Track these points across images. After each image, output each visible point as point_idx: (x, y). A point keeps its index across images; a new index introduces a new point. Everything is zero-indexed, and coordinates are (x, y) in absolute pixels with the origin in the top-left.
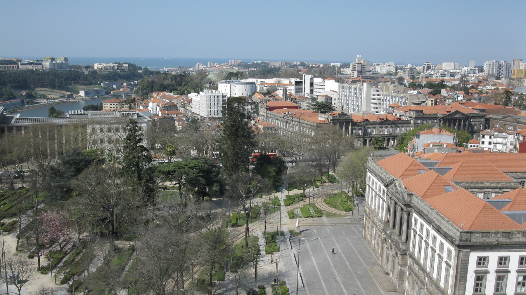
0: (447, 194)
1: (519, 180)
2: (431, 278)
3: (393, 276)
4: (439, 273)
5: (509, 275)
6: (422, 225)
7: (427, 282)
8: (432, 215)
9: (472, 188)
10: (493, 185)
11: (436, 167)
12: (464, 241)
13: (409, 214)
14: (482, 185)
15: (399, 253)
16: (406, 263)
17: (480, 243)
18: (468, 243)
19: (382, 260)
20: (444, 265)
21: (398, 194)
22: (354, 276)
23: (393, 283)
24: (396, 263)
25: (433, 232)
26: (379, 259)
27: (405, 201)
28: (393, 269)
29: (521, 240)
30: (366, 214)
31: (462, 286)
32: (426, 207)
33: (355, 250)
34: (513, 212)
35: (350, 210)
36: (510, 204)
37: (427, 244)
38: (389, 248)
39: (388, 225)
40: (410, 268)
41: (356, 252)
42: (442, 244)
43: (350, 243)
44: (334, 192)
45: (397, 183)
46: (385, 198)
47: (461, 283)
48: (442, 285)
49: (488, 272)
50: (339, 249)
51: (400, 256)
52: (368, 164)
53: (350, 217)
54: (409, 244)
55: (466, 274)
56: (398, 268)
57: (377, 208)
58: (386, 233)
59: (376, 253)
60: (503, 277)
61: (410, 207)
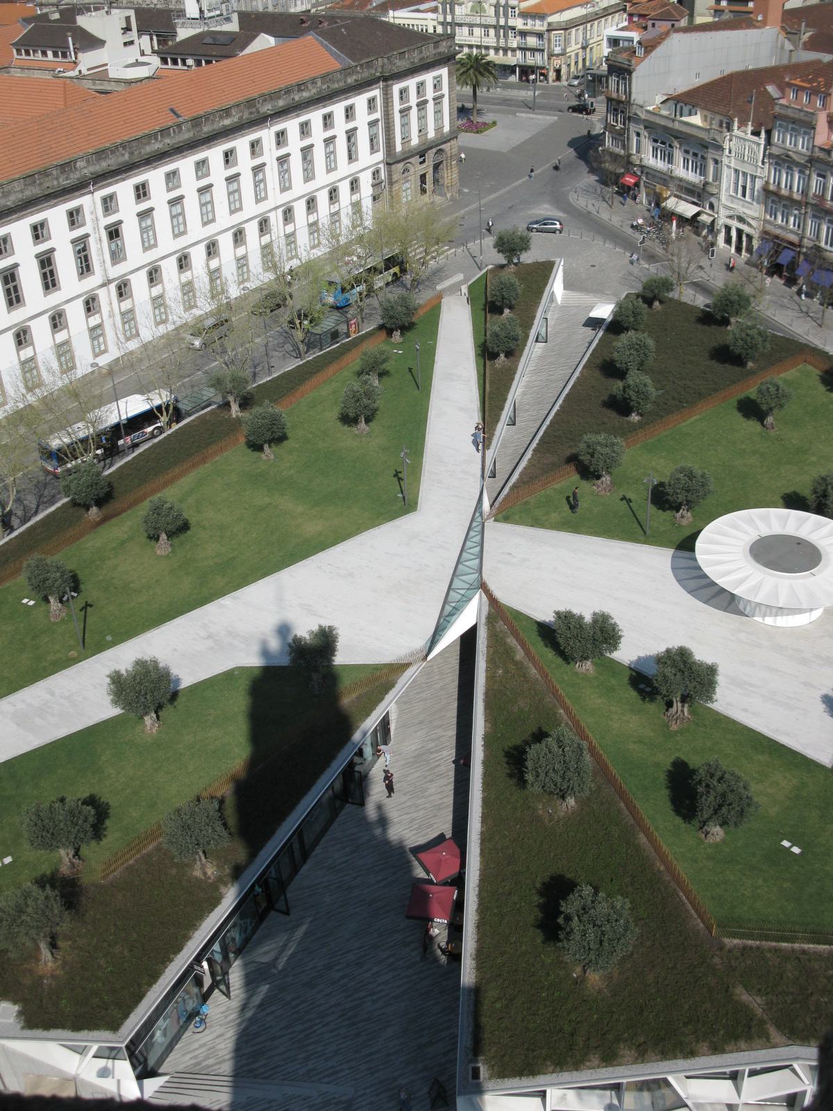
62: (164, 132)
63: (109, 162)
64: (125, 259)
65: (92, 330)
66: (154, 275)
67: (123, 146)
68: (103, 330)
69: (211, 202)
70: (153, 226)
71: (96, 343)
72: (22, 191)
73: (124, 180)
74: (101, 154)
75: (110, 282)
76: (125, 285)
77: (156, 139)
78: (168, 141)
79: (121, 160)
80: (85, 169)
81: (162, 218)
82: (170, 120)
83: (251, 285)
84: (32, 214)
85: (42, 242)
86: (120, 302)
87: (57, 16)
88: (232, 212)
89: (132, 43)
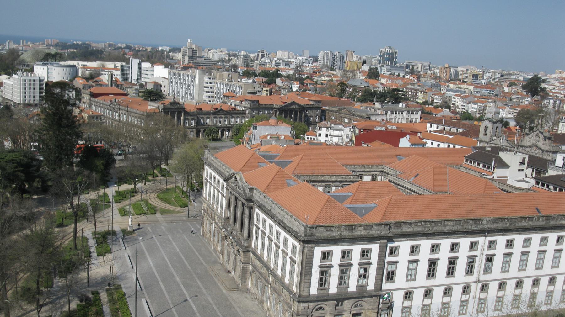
0: (289, 188)
1: (358, 173)
2: (275, 275)
3: (235, 275)
4: (283, 270)
5: (352, 267)
6: (264, 221)
7: (271, 279)
8: (276, 210)
9: (313, 181)
10: (333, 179)
11: (276, 160)
12: (309, 236)
13: (251, 209)
14: (323, 179)
15: (241, 250)
16: (249, 260)
17: (324, 237)
18: (313, 238)
19: (223, 258)
20: (288, 261)
21: (239, 188)
22: (194, 275)
23: (235, 282)
24: (238, 260)
25: (276, 228)
26: (219, 258)
27: (246, 196)
28: (235, 266)
29: (362, 233)
30: (204, 210)
31: (307, 281)
32: (269, 202)
33: (193, 248)
34: (355, 206)
35: (185, 206)
36: (351, 198)
37: (270, 240)
38: (230, 245)
39: (229, 221)
40: (253, 265)
41: (195, 250)
42: (286, 240)
43: (188, 241)
44: (168, 187)
45: (237, 177)
46: (225, 193)
47: (306, 278)
48: (287, 281)
49: (332, 266)
50: (176, 247)
51: (242, 253)
52: (206, 157)
53: (186, 213)
54: (251, 241)
55: (311, 269)
56: (240, 265)
57: (215, 203)
58: (227, 230)
59: (216, 250)
60: (346, 270)
61: (252, 201)
62: (530, 218)
63: (499, 225)
64: (490, 273)
65: (462, 301)
66: (502, 286)
67: (508, 219)
68: (468, 304)
69: (543, 259)
70: (509, 262)
71: (462, 308)
72: (453, 226)
73: (503, 235)
74: (496, 220)
75: (479, 281)
76: (486, 286)
77: (525, 221)
78: (531, 223)
79: (505, 225)
80: (486, 225)
81: (515, 260)
82: (535, 214)
83: (553, 307)
84: (454, 238)
85: (454, 252)
86: (480, 293)
87: (489, 149)
88: (552, 267)
89: (523, 170)
